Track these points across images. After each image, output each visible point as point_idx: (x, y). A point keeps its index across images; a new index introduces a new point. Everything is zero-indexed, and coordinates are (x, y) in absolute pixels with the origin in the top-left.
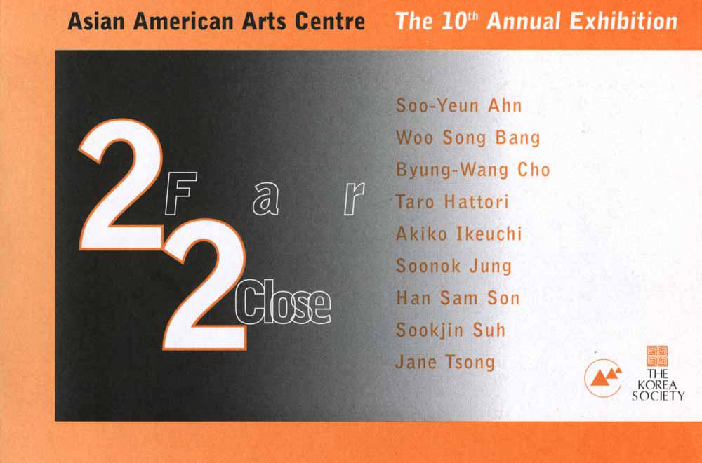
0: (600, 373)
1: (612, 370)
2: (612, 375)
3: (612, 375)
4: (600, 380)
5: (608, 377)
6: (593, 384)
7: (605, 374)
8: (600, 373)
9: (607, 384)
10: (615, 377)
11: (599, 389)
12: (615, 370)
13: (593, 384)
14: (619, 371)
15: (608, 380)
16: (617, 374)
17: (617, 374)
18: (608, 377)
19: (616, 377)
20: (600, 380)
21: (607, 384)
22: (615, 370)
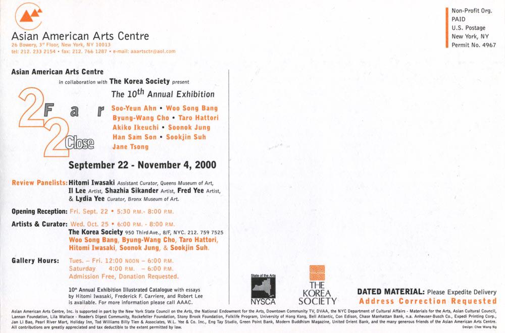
0: (26, 13)
2: (35, 14)
3: (35, 14)
4: (26, 18)
8: (26, 13)
10: (38, 16)
11: (26, 25)
12: (37, 10)
14: (40, 11)
15: (33, 18)
16: (39, 14)
17: (39, 14)
19: (38, 16)
20: (26, 18)
21: (31, 20)
22: (37, 10)
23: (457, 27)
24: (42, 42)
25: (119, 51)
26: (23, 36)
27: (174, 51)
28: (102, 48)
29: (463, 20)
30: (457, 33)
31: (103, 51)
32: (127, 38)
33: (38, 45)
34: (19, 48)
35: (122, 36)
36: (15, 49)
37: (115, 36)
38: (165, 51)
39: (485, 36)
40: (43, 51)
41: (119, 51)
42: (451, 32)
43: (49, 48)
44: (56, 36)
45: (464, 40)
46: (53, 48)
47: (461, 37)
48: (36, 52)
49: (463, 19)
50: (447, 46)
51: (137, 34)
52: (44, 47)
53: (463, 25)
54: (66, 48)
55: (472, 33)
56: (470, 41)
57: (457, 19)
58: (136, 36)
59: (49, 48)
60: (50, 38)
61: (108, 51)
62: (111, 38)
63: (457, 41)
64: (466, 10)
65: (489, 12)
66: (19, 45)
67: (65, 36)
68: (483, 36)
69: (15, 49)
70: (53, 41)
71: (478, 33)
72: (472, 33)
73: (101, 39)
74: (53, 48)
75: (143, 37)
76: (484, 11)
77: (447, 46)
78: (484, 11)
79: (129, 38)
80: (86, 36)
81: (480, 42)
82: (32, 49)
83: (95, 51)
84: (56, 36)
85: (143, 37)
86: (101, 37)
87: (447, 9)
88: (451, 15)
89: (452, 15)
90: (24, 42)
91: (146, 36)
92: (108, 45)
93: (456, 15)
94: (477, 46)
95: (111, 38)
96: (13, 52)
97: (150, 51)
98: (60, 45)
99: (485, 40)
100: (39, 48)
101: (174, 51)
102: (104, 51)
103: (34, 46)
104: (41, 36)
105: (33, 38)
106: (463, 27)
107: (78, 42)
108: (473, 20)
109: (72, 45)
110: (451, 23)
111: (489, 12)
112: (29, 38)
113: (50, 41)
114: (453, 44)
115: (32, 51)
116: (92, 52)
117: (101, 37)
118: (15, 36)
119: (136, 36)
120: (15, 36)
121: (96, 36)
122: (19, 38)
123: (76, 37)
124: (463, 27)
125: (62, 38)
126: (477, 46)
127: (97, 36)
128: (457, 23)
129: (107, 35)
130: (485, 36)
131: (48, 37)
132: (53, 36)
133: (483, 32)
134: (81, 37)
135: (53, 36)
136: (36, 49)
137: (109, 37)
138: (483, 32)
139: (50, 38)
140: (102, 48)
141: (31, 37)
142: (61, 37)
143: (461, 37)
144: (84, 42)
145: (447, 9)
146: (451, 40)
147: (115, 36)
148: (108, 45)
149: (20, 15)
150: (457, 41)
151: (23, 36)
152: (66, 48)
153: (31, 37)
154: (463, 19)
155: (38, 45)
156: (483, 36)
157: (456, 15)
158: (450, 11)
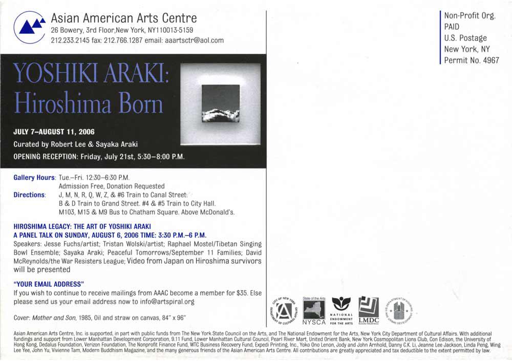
5: (33, 27)
7: (32, 25)
18: (33, 27)
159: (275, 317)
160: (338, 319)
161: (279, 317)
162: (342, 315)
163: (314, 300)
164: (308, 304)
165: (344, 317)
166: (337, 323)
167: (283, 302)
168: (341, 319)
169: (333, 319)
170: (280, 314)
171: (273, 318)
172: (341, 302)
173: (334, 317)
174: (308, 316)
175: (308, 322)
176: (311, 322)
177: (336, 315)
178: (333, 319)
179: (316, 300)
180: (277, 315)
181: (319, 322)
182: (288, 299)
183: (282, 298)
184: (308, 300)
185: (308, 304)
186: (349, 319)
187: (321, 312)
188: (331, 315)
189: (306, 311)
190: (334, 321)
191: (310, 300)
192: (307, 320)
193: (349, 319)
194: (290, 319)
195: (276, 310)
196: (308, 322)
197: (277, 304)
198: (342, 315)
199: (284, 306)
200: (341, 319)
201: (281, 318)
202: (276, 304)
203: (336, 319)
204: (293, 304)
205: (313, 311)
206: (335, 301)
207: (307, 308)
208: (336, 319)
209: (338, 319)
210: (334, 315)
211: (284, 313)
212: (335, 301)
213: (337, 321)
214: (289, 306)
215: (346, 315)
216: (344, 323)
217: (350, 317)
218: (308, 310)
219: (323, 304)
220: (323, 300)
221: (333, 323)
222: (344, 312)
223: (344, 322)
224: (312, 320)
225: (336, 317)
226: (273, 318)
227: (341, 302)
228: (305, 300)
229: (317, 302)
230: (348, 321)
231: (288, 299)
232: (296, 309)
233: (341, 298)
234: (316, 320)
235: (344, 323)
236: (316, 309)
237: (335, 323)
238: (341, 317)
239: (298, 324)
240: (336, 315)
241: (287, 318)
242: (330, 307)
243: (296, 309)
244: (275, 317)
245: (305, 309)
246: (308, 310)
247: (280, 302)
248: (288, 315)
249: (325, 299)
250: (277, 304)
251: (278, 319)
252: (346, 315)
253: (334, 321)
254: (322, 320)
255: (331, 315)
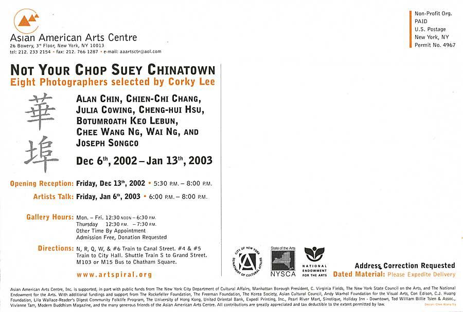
1: (32, 15)
2: (32, 19)
3: (32, 19)
4: (24, 22)
5: (30, 20)
6: (19, 25)
7: (28, 20)
9: (29, 25)
11: (25, 29)
12: (34, 16)
13: (19, 25)
14: (37, 16)
15: (30, 22)
16: (36, 19)
17: (36, 19)
18: (30, 20)
20: (24, 22)
21: (29, 25)
22: (34, 16)
23: (420, 29)
24: (39, 43)
25: (109, 52)
26: (21, 38)
27: (160, 51)
28: (95, 49)
29: (426, 21)
30: (420, 34)
31: (94, 51)
32: (117, 39)
33: (35, 46)
34: (17, 49)
35: (112, 37)
36: (13, 49)
37: (106, 38)
38: (152, 51)
39: (446, 37)
40: (39, 52)
41: (109, 52)
42: (414, 33)
43: (46, 48)
44: (52, 38)
45: (427, 41)
46: (48, 49)
47: (423, 38)
48: (33, 52)
49: (425, 21)
50: (411, 47)
51: (126, 36)
52: (41, 48)
53: (425, 26)
54: (60, 49)
55: (433, 34)
56: (432, 41)
57: (419, 21)
58: (125, 37)
59: (46, 48)
60: (46, 40)
61: (99, 51)
62: (102, 39)
63: (420, 41)
64: (428, 13)
65: (449, 14)
66: (17, 46)
67: (59, 38)
68: (443, 37)
69: (13, 49)
70: (49, 43)
71: (439, 34)
72: (433, 34)
73: (92, 39)
74: (48, 49)
75: (131, 38)
76: (444, 13)
77: (411, 47)
78: (444, 13)
79: (119, 39)
80: (79, 38)
81: (441, 42)
82: (28, 49)
83: (87, 52)
84: (52, 38)
85: (131, 38)
86: (92, 39)
87: (410, 12)
88: (414, 17)
89: (415, 17)
90: (21, 43)
91: (135, 38)
92: (101, 46)
93: (419, 17)
94: (438, 46)
95: (102, 39)
96: (12, 52)
97: (138, 52)
98: (56, 46)
99: (446, 41)
100: (35, 49)
101: (160, 51)
102: (96, 52)
103: (31, 47)
104: (37, 38)
105: (30, 39)
106: (425, 28)
107: (71, 42)
108: (433, 21)
109: (68, 46)
110: (414, 25)
111: (449, 14)
112: (27, 39)
113: (46, 42)
114: (416, 44)
115: (28, 51)
116: (84, 52)
117: (92, 39)
118: (13, 37)
119: (125, 37)
120: (13, 38)
121: (88, 37)
122: (17, 39)
123: (69, 38)
124: (425, 28)
125: (57, 40)
126: (438, 46)
127: (89, 37)
128: (419, 25)
129: (98, 36)
130: (446, 37)
131: (44, 39)
132: (48, 38)
133: (444, 33)
134: (74, 38)
135: (48, 38)
136: (33, 49)
137: (100, 39)
138: (444, 33)
139: (46, 40)
140: (95, 49)
141: (28, 39)
142: (55, 38)
143: (423, 38)
144: (79, 43)
145: (410, 12)
146: (414, 41)
147: (106, 38)
148: (101, 46)
149: (19, 20)
150: (420, 41)
151: (21, 38)
152: (60, 49)
153: (28, 39)
154: (425, 21)
155: (35, 46)
156: (443, 37)
157: (419, 17)
158: (413, 14)
159: (238, 268)
160: (311, 271)
161: (242, 268)
162: (316, 266)
163: (283, 250)
164: (276, 254)
165: (317, 268)
166: (310, 275)
167: (247, 252)
168: (314, 271)
169: (306, 271)
170: (243, 266)
171: (235, 269)
172: (314, 252)
173: (305, 268)
174: (275, 267)
175: (276, 274)
176: (280, 274)
177: (309, 266)
178: (306, 271)
179: (286, 250)
180: (240, 266)
181: (288, 274)
182: (251, 248)
183: (245, 248)
184: (276, 250)
185: (276, 254)
186: (323, 271)
187: (290, 263)
188: (304, 266)
189: (274, 262)
190: (307, 273)
191: (279, 250)
192: (276, 272)
193: (323, 271)
194: (254, 271)
195: (238, 260)
196: (276, 274)
197: (240, 254)
198: (316, 266)
199: (248, 256)
200: (314, 271)
201: (244, 269)
202: (238, 254)
203: (309, 271)
204: (257, 255)
205: (282, 262)
206: (308, 251)
207: (276, 259)
208: (309, 271)
209: (311, 271)
210: (307, 266)
211: (247, 263)
212: (308, 251)
213: (310, 273)
214: (253, 256)
215: (319, 266)
216: (317, 275)
217: (324, 268)
218: (277, 261)
219: (292, 254)
220: (292, 250)
221: (306, 275)
222: (317, 263)
223: (318, 273)
224: (281, 271)
225: (309, 268)
226: (235, 269)
227: (314, 252)
228: (273, 250)
229: (286, 252)
230: (322, 273)
231: (251, 248)
232: (261, 259)
233: (315, 248)
234: (285, 271)
235: (317, 275)
236: (286, 260)
237: (308, 275)
238: (314, 268)
239: (264, 276)
240: (309, 266)
241: (251, 269)
242: (301, 259)
243: (261, 259)
244: (238, 268)
245: (273, 260)
246: (277, 261)
247: (243, 252)
248: (252, 266)
249: (294, 248)
250: (240, 254)
251: (241, 270)
252: (319, 266)
253: (307, 273)
254: (291, 272)
255: (304, 266)
